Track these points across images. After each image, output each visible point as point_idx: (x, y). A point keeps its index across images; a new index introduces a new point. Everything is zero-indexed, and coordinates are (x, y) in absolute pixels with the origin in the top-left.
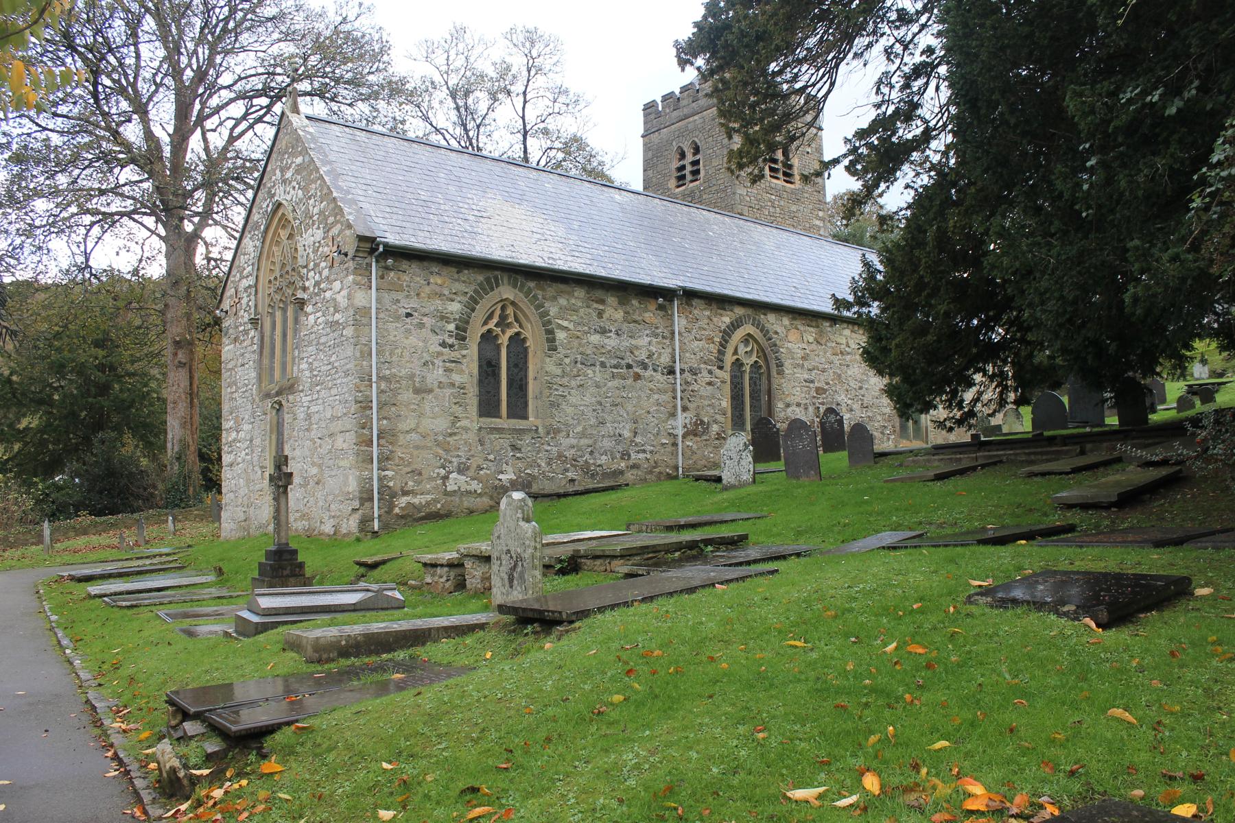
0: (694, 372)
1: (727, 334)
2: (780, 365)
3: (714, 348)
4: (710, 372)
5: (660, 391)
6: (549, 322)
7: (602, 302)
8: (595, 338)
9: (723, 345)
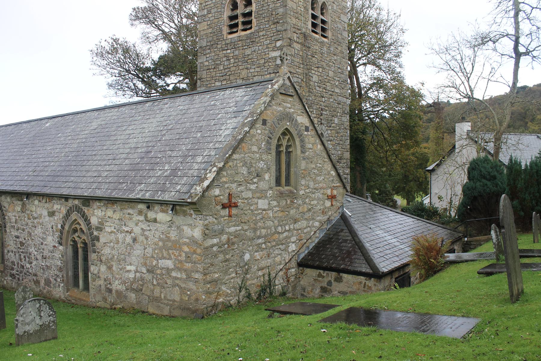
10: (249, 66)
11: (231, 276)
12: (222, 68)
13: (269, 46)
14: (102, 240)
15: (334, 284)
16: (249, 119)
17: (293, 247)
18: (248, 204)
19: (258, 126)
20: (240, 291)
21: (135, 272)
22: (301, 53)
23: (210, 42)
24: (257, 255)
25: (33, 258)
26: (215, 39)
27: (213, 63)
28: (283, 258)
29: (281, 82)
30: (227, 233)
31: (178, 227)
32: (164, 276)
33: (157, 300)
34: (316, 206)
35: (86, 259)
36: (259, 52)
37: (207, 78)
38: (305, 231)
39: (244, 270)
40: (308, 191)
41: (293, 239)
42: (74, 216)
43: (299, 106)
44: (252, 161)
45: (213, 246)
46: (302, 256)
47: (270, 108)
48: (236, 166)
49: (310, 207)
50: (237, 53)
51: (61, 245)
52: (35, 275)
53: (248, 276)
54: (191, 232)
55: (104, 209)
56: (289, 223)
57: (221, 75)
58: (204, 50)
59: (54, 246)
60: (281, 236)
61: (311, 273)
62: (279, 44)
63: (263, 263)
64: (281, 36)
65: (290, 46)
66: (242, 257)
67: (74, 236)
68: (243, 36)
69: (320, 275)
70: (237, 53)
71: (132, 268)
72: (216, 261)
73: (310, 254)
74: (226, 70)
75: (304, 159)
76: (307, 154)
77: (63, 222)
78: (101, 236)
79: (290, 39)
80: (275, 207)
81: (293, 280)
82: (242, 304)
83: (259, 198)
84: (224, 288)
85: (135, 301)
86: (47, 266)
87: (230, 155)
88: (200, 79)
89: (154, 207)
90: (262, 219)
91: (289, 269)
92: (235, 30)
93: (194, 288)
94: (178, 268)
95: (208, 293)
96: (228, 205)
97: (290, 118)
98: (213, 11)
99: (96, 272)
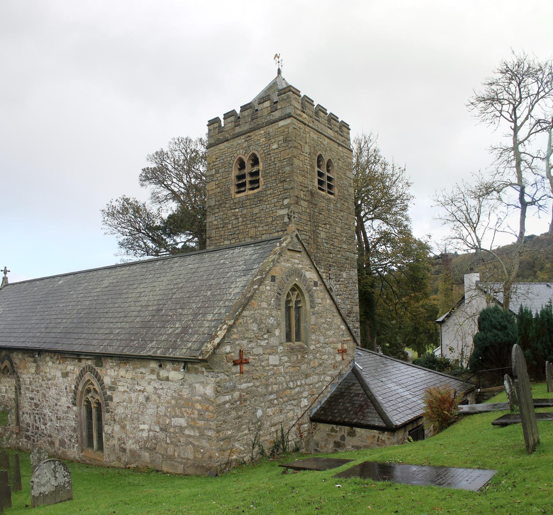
10: (257, 225)
11: (244, 433)
12: (231, 227)
13: (277, 204)
14: (115, 400)
15: (347, 438)
16: (258, 277)
17: (305, 402)
18: (259, 360)
19: (267, 282)
20: (253, 448)
21: (149, 431)
22: (308, 211)
23: (219, 201)
24: (270, 411)
25: (48, 419)
26: (223, 198)
27: (222, 222)
28: (296, 414)
29: (289, 240)
30: (239, 390)
31: (190, 385)
32: (177, 435)
33: (171, 458)
34: (327, 360)
35: (99, 419)
36: (267, 210)
37: (216, 237)
38: (317, 386)
39: (257, 426)
40: (318, 345)
41: (305, 394)
42: (88, 376)
43: (307, 262)
44: (262, 318)
45: (225, 403)
46: (314, 411)
47: (278, 264)
48: (246, 322)
49: (321, 362)
50: (245, 211)
51: (75, 406)
52: (50, 436)
53: (261, 432)
54: (203, 390)
55: (116, 369)
56: (301, 378)
57: (230, 233)
58: (213, 209)
59: (69, 407)
60: (293, 392)
61: (325, 428)
62: (286, 202)
63: (276, 419)
64: (288, 194)
65: (297, 204)
66: (254, 413)
67: (88, 397)
68: (251, 195)
69: (333, 430)
70: (245, 211)
71: (146, 427)
72: (229, 418)
73: (322, 408)
74: (235, 229)
75: (314, 314)
76: (316, 309)
77: (77, 382)
78: (114, 396)
79: (297, 197)
80: (286, 362)
81: (306, 435)
82: (256, 461)
83: (269, 354)
84: (237, 445)
85: (148, 460)
86: (61, 427)
87: (239, 313)
88: (209, 238)
89: (166, 366)
90: (273, 375)
91: (302, 424)
92: (243, 189)
93: (207, 445)
94: (191, 426)
95: (222, 450)
96: (239, 362)
97: (299, 273)
98: (221, 171)
99: (109, 432)
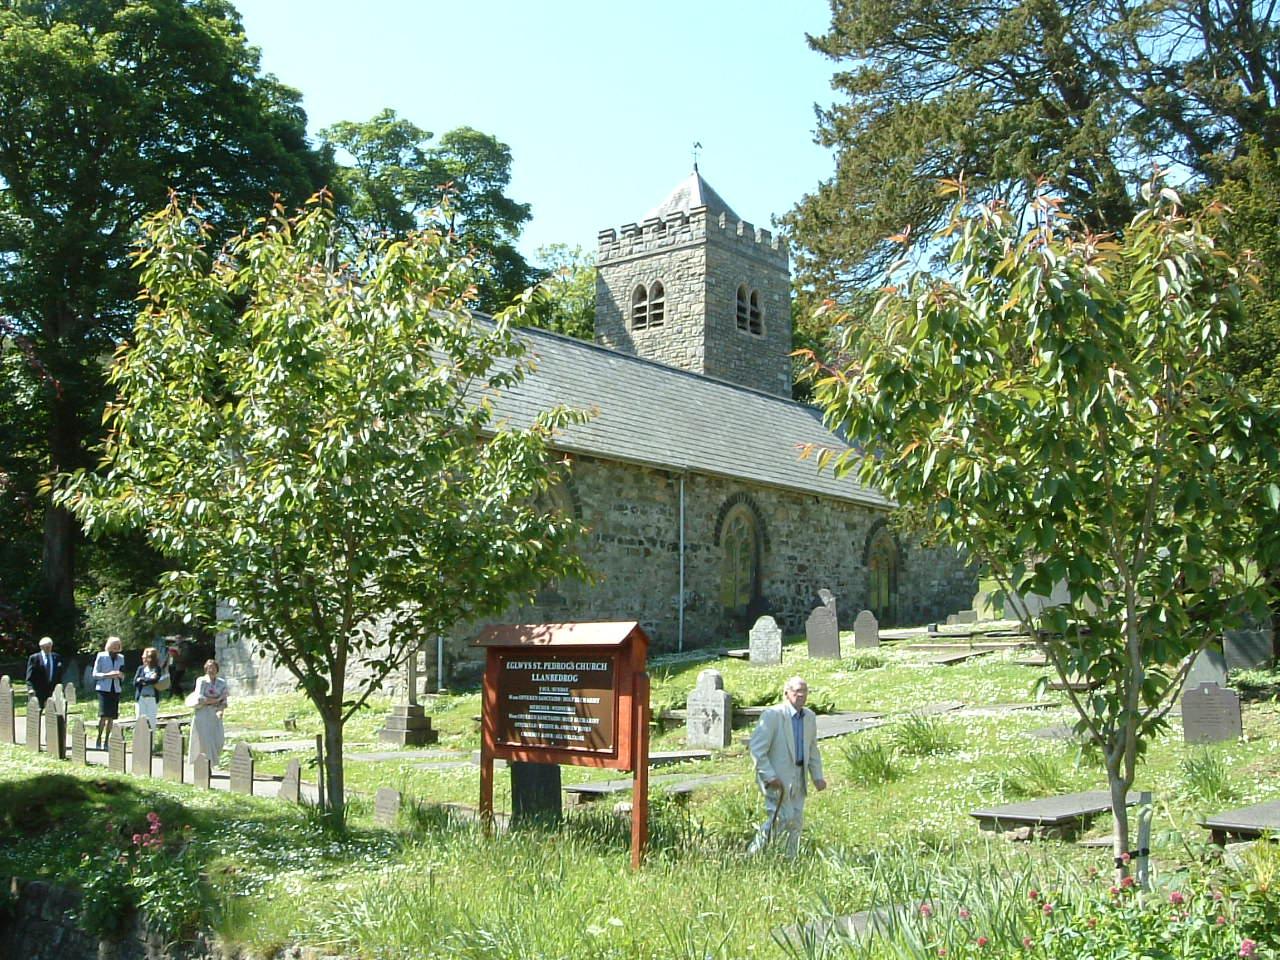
0: (695, 548)
1: (723, 512)
2: (767, 542)
3: (712, 525)
4: (708, 549)
5: (666, 566)
6: (578, 500)
7: (621, 480)
8: (614, 516)
9: (720, 523)
71: (934, 582)
